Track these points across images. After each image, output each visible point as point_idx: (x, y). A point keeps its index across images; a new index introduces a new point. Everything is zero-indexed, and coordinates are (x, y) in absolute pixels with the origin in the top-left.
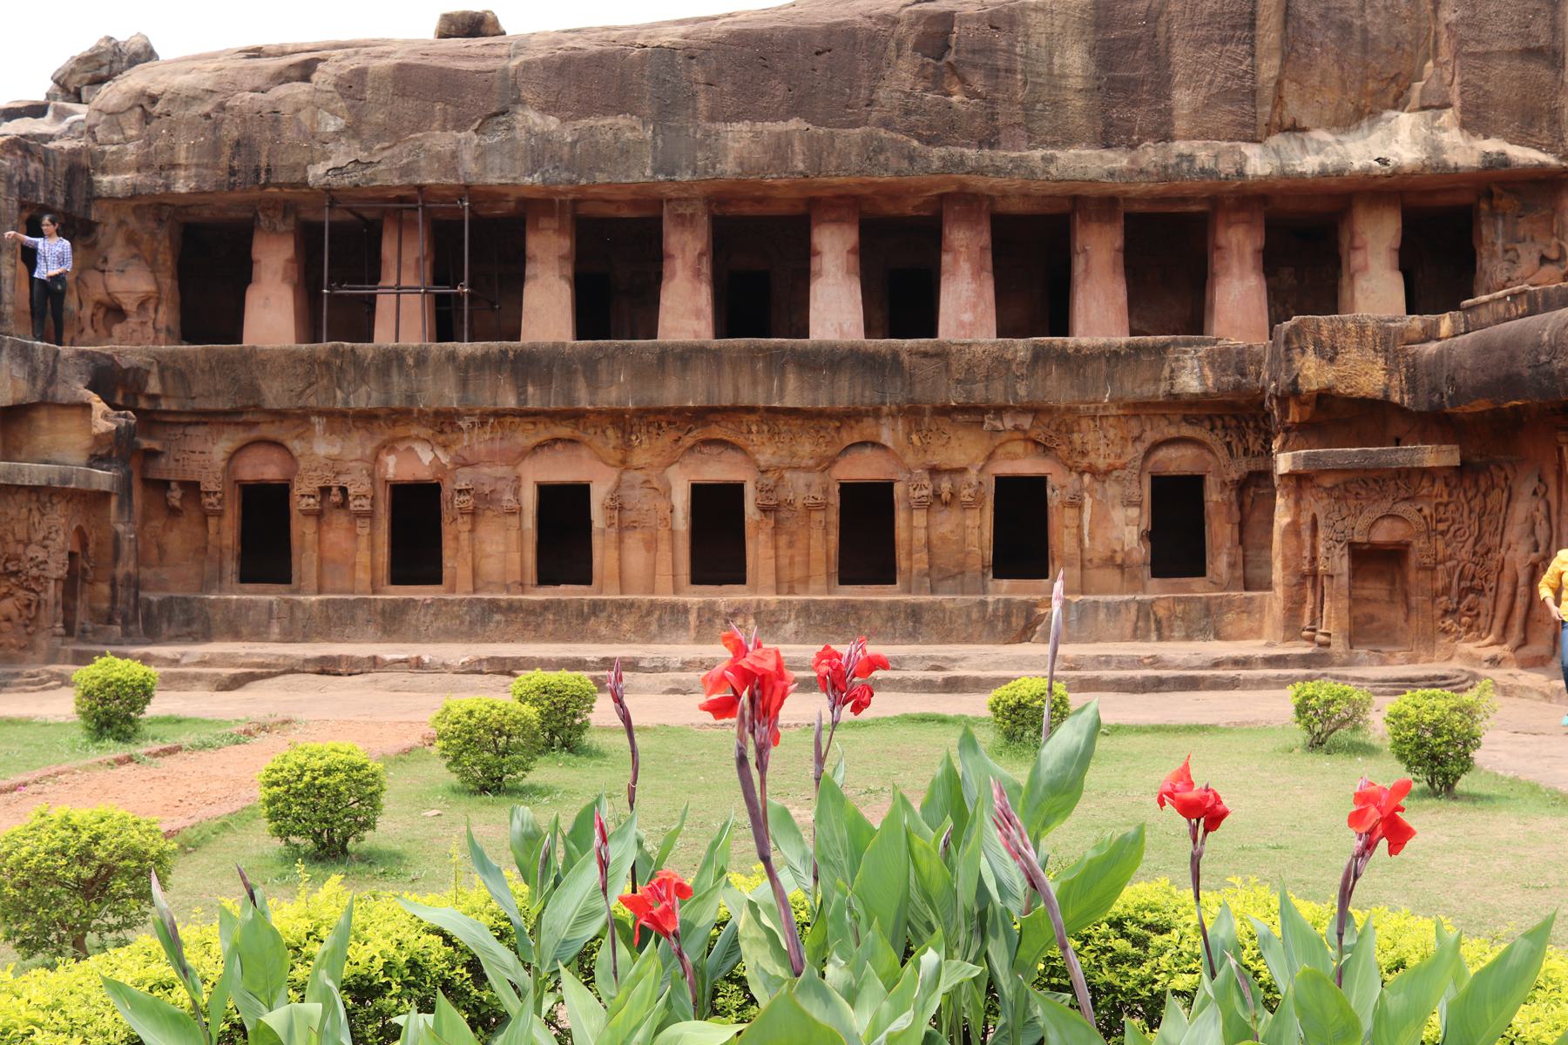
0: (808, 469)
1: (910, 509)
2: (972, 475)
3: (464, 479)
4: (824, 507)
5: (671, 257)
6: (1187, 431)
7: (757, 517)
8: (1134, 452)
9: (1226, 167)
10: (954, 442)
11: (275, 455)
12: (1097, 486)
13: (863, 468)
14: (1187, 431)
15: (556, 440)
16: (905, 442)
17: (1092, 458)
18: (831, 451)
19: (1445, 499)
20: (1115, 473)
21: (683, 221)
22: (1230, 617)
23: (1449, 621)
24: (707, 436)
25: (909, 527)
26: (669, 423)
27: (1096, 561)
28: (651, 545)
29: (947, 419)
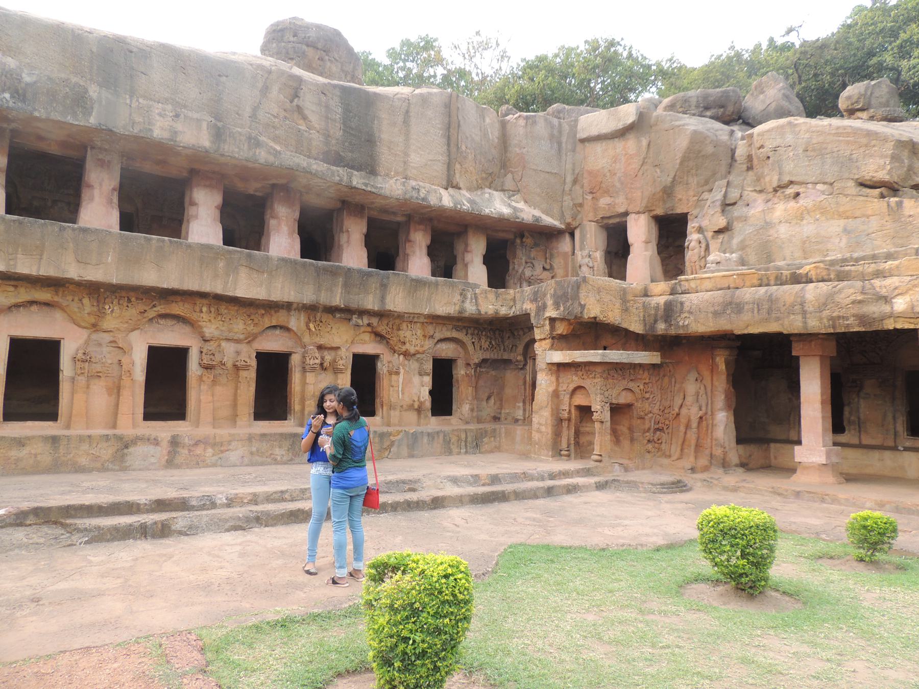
0: (238, 341)
1: (304, 370)
2: (343, 350)
4: (246, 368)
5: (90, 186)
6: (455, 334)
7: (199, 373)
9: (433, 201)
10: (334, 331)
12: (406, 362)
13: (274, 344)
14: (455, 334)
15: (32, 303)
16: (304, 328)
17: (407, 346)
18: (256, 330)
19: (647, 381)
20: (418, 356)
21: (102, 164)
22: (486, 440)
23: (650, 446)
24: (168, 311)
26: (137, 299)
27: (405, 406)
28: (116, 390)
29: (330, 316)
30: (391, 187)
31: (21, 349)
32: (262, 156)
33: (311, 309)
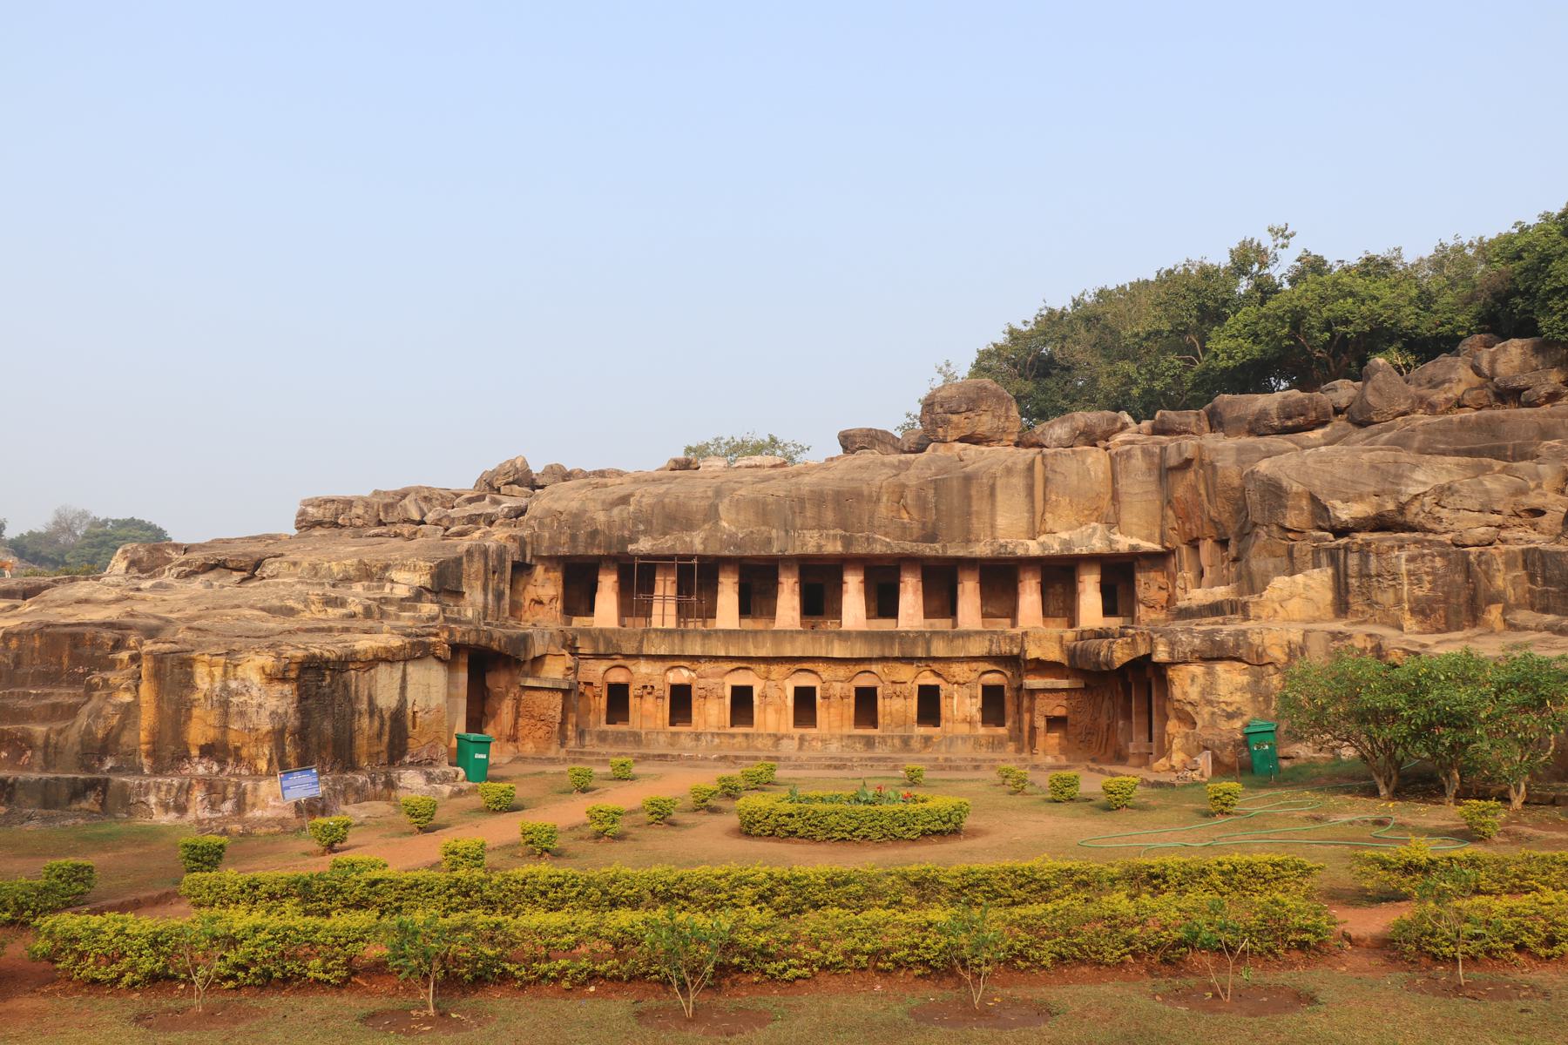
3: (702, 683)
8: (974, 675)
9: (1020, 552)
11: (623, 671)
13: (865, 681)
28: (778, 711)
30: (981, 549)
31: (736, 690)
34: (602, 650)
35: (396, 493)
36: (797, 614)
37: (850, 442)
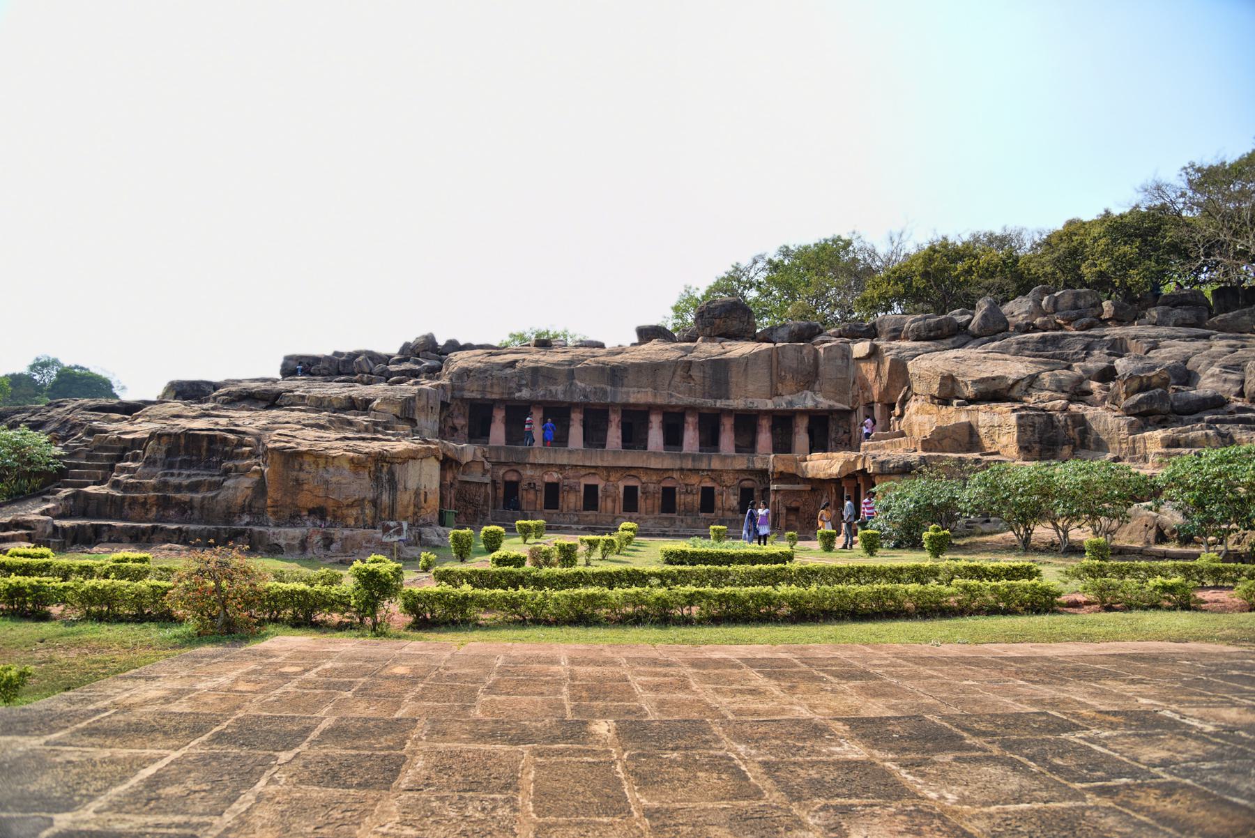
3: (566, 482)
8: (736, 482)
13: (668, 484)
21: (615, 412)
25: (680, 499)
28: (614, 501)
32: (674, 401)
33: (681, 470)
34: (503, 460)
35: (350, 354)
36: (620, 441)
37: (646, 334)
